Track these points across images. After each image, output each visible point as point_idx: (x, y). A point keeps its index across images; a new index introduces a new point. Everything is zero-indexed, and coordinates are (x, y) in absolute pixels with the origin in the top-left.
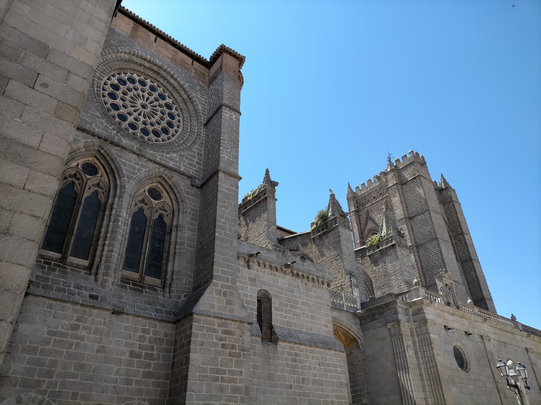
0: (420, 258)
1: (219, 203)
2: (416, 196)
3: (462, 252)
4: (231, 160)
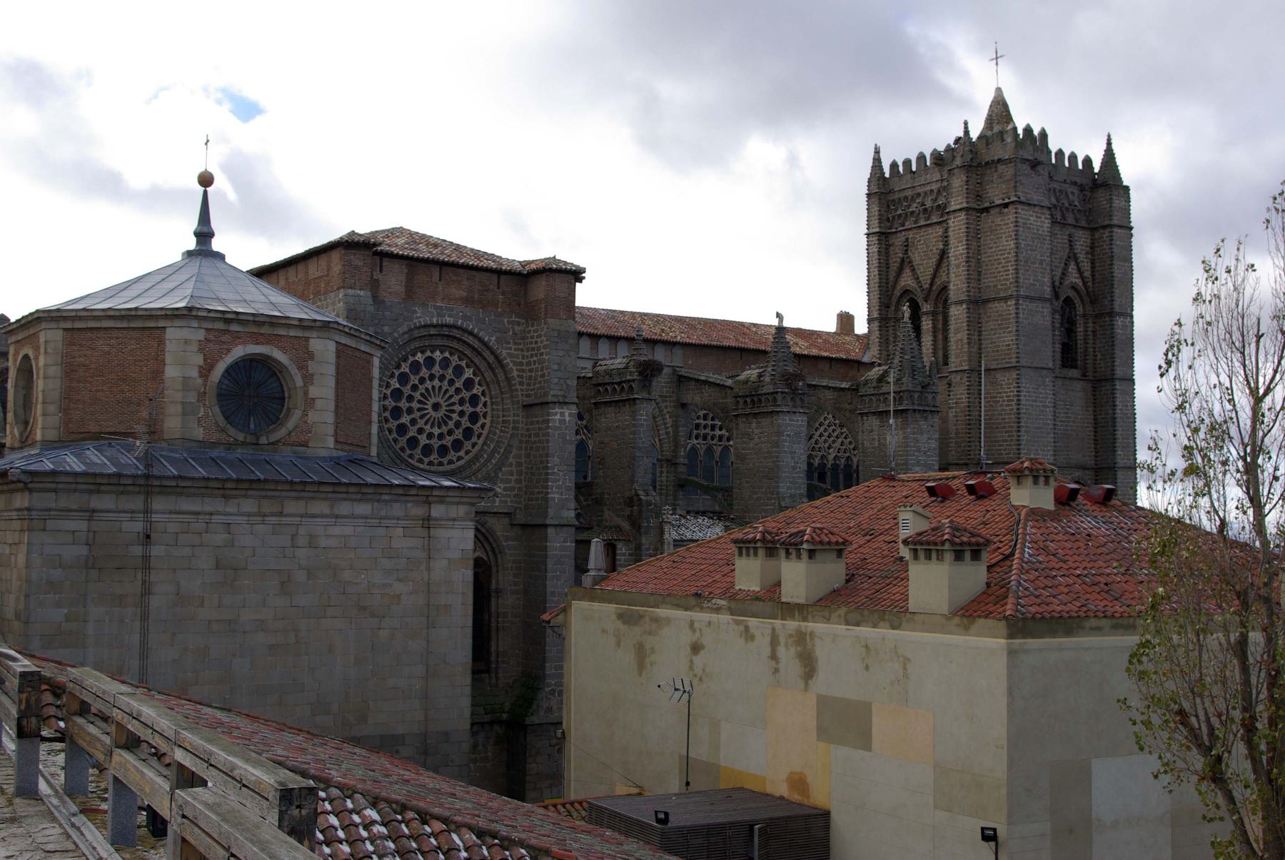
2: (1000, 250)
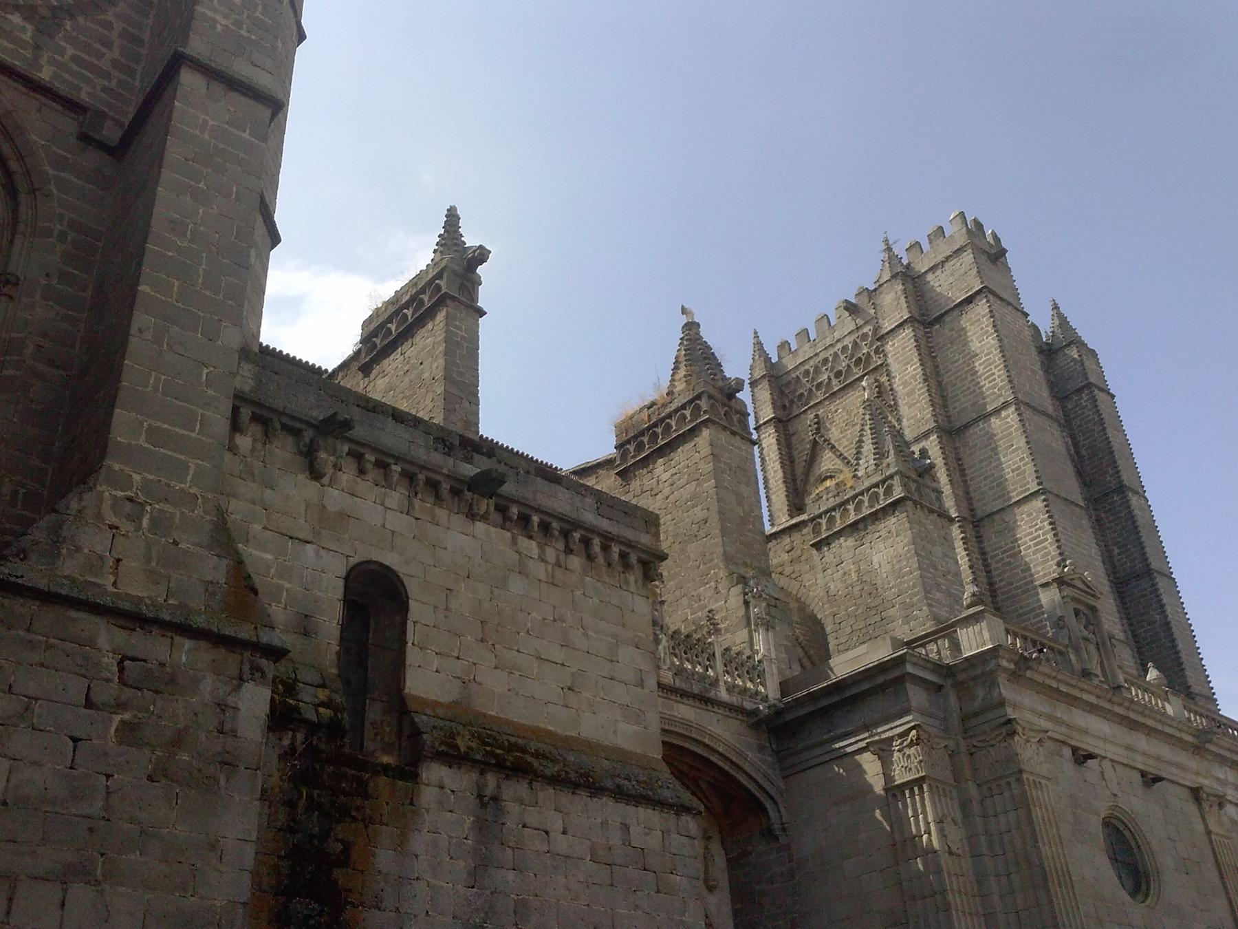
0: (985, 560)
1: (166, 174)
3: (1119, 548)
4: (244, 33)
